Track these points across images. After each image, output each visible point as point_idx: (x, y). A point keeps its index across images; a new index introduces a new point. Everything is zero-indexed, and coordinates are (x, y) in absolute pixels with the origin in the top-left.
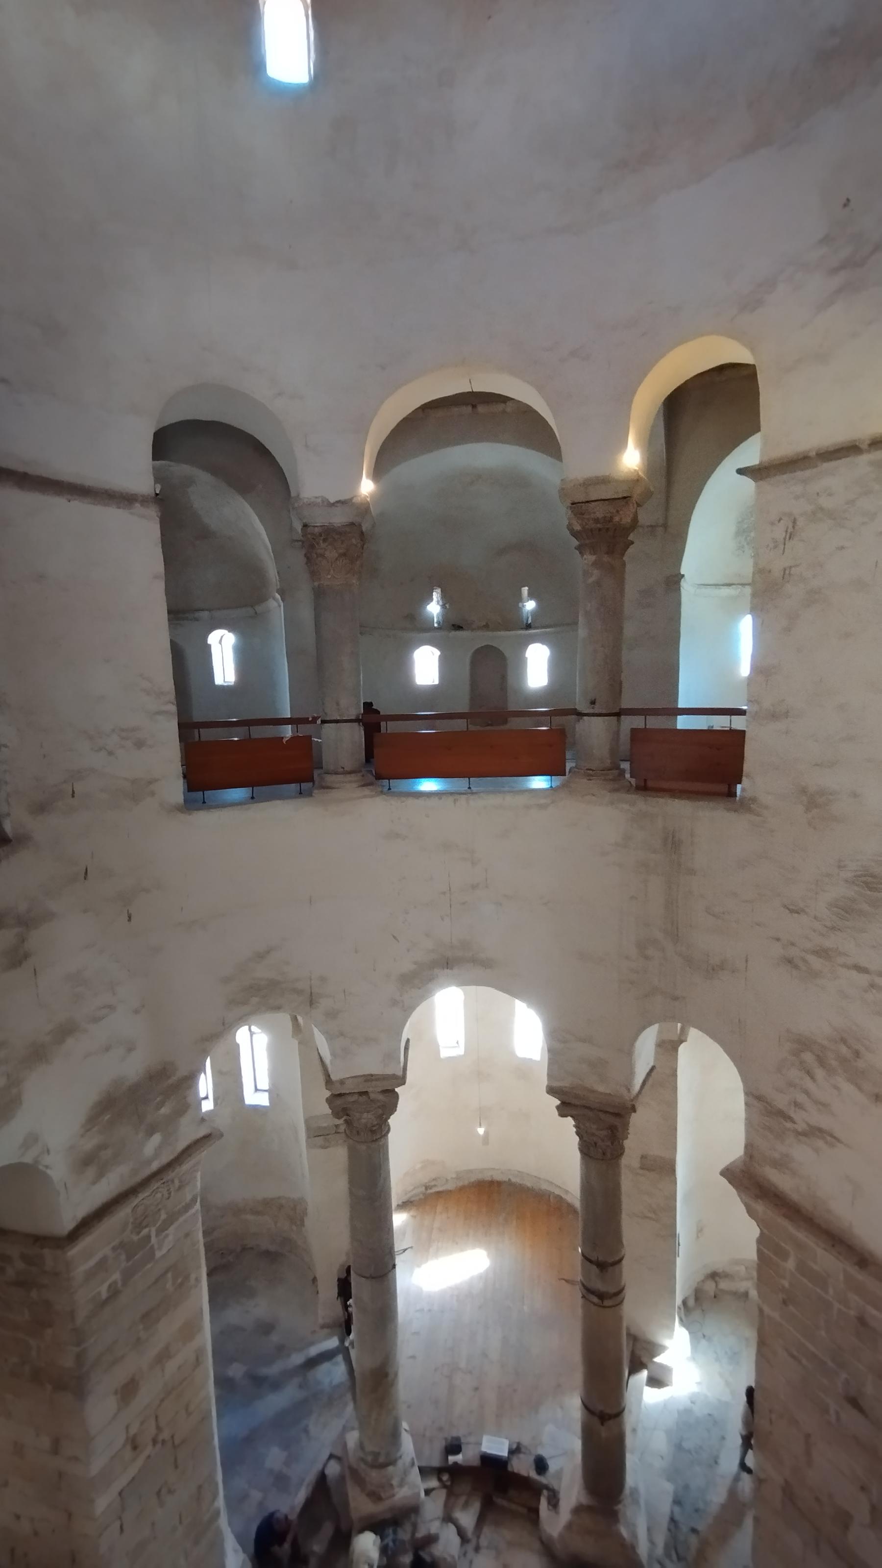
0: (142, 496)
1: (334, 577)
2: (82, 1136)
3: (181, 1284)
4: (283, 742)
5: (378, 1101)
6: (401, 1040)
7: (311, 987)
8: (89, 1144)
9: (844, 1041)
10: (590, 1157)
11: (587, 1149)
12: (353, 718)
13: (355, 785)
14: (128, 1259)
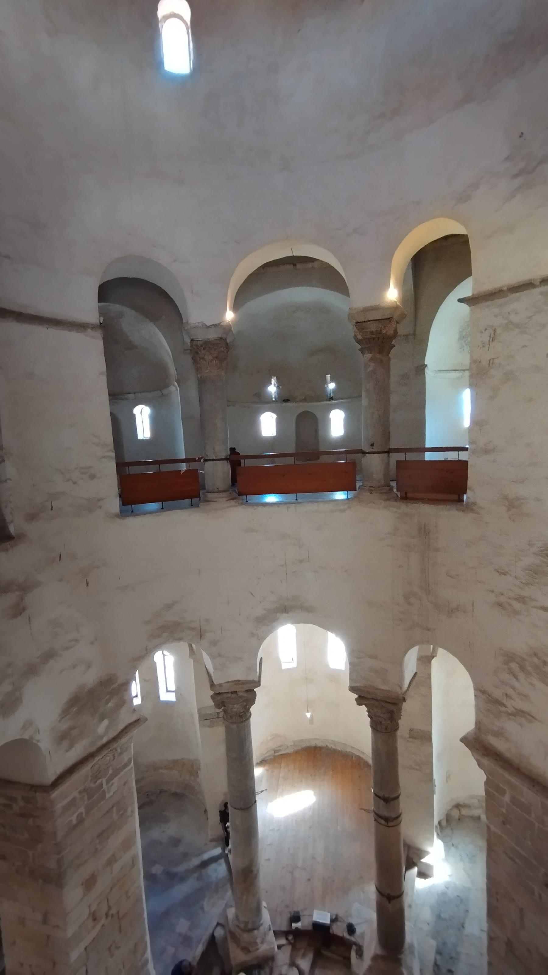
0: (92, 325)
1: (211, 372)
2: (60, 721)
3: (122, 815)
4: (181, 474)
5: (243, 697)
6: (257, 659)
7: (200, 626)
8: (64, 726)
9: (536, 655)
10: (377, 731)
11: (375, 725)
12: (224, 457)
13: (225, 499)
14: (89, 798)
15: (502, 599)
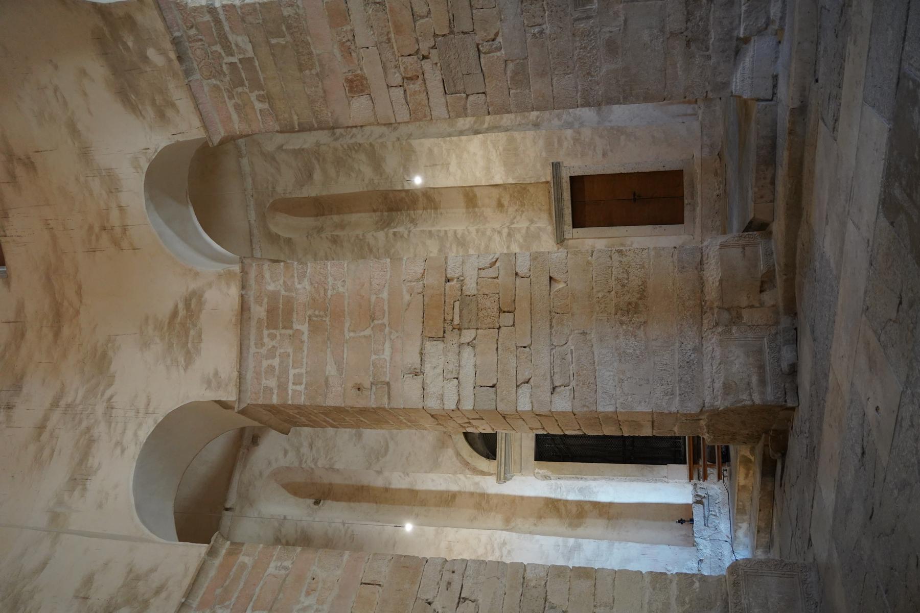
2: (144, 118)
8: (150, 112)
14: (243, 85)
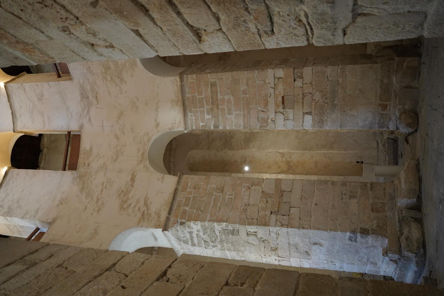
9: (120, 195)
15: (96, 209)
